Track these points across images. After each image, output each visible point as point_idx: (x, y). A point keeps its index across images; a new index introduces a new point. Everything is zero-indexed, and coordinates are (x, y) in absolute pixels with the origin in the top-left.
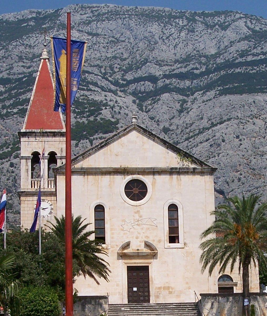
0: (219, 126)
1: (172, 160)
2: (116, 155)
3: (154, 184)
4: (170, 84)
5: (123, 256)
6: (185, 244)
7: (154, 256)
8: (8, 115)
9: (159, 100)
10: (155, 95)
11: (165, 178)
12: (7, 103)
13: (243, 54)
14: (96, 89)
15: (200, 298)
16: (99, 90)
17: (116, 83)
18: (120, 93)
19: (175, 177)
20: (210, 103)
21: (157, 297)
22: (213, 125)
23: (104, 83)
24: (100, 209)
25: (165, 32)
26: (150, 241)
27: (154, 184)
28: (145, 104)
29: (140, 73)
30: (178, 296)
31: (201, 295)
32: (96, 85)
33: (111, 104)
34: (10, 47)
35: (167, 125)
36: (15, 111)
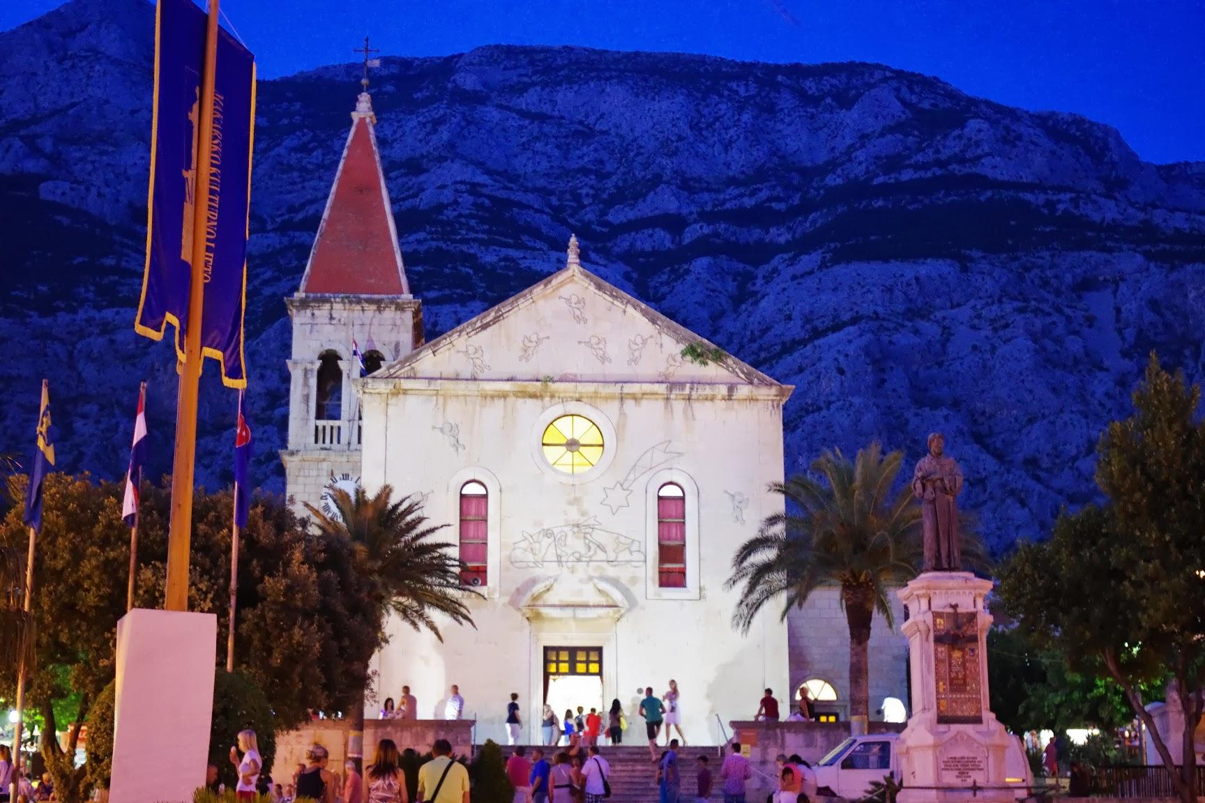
0: (832, 338)
4: (716, 234)
9: (688, 272)
13: (892, 163)
14: (539, 244)
15: (731, 733)
20: (811, 282)
22: (817, 334)
25: (706, 111)
27: (620, 430)
29: (644, 209)
31: (734, 724)
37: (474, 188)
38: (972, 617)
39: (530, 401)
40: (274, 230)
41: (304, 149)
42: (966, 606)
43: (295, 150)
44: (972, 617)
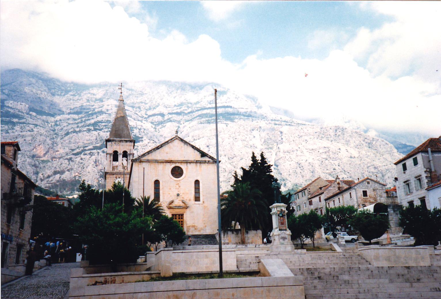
0: (198, 140)
2: (167, 153)
3: (187, 169)
5: (170, 208)
6: (203, 202)
7: (187, 208)
8: (80, 131)
9: (165, 126)
11: (193, 165)
12: (80, 125)
16: (133, 120)
19: (198, 164)
21: (188, 231)
24: (157, 183)
26: (185, 199)
27: (187, 169)
28: (157, 128)
29: (156, 111)
30: (199, 231)
33: (140, 127)
34: (82, 94)
36: (85, 129)
39: (168, 164)
40: (67, 114)
41: (74, 95)
43: (71, 95)
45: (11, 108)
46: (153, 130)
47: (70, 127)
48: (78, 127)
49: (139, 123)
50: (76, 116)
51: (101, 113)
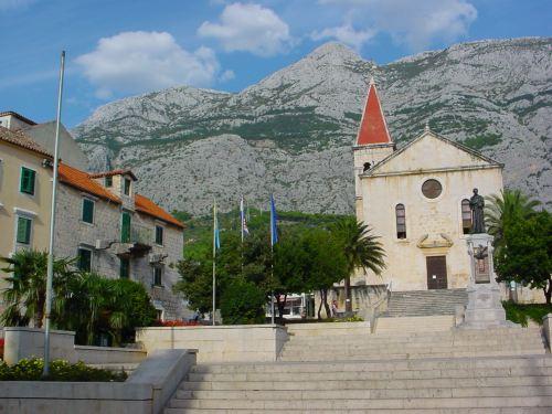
1: (464, 158)
7: (450, 245)
10: (532, 110)
12: (411, 128)
17: (499, 104)
18: (503, 112)
19: (466, 173)
21: (454, 283)
23: (489, 104)
24: (400, 207)
27: (447, 183)
29: (517, 94)
32: (481, 106)
33: (495, 121)
35: (544, 135)
37: (459, 93)
38: (486, 248)
41: (400, 86)
42: (484, 245)
44: (486, 248)
45: (322, 116)
46: (516, 122)
47: (398, 133)
48: (408, 131)
49: (494, 114)
50: (405, 116)
51: (439, 106)
